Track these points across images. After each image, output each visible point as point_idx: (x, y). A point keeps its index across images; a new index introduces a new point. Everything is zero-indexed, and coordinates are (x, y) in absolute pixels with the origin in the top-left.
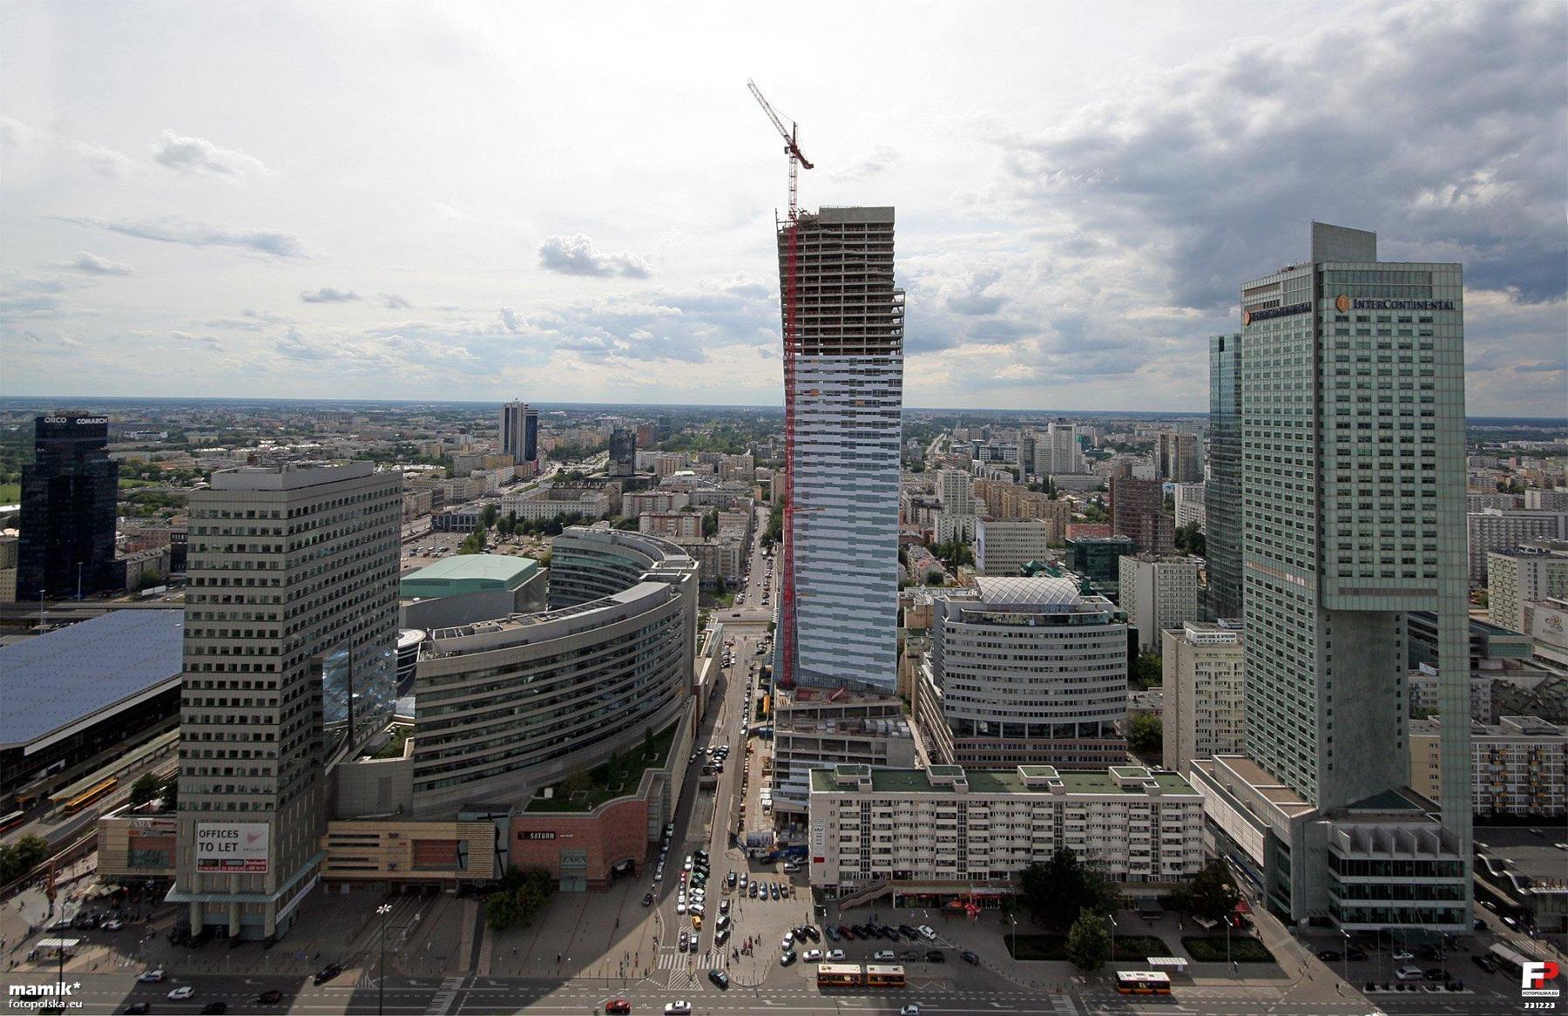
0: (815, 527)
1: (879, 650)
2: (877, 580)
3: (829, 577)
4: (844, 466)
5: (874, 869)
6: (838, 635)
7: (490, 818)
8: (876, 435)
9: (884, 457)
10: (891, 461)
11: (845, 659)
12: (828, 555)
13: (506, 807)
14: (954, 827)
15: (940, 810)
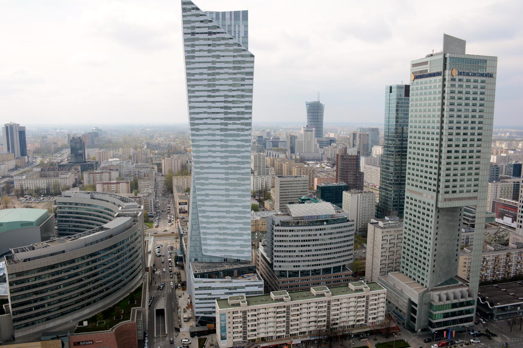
0: (207, 184)
1: (242, 243)
2: (241, 209)
3: (216, 209)
4: (222, 152)
5: (248, 338)
6: (222, 237)
7: (58, 338)
8: (238, 135)
9: (243, 146)
10: (246, 149)
11: (226, 248)
12: (215, 198)
13: (65, 332)
14: (284, 317)
15: (278, 310)
